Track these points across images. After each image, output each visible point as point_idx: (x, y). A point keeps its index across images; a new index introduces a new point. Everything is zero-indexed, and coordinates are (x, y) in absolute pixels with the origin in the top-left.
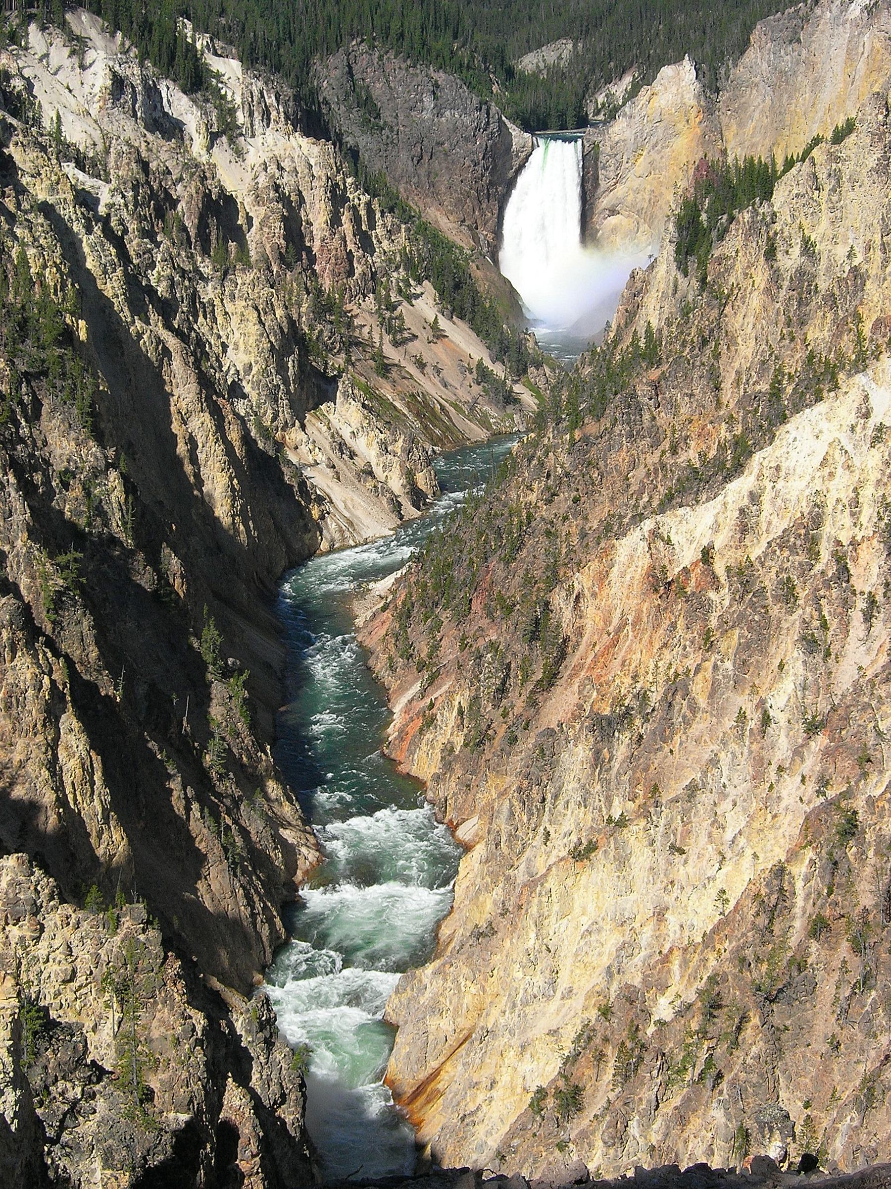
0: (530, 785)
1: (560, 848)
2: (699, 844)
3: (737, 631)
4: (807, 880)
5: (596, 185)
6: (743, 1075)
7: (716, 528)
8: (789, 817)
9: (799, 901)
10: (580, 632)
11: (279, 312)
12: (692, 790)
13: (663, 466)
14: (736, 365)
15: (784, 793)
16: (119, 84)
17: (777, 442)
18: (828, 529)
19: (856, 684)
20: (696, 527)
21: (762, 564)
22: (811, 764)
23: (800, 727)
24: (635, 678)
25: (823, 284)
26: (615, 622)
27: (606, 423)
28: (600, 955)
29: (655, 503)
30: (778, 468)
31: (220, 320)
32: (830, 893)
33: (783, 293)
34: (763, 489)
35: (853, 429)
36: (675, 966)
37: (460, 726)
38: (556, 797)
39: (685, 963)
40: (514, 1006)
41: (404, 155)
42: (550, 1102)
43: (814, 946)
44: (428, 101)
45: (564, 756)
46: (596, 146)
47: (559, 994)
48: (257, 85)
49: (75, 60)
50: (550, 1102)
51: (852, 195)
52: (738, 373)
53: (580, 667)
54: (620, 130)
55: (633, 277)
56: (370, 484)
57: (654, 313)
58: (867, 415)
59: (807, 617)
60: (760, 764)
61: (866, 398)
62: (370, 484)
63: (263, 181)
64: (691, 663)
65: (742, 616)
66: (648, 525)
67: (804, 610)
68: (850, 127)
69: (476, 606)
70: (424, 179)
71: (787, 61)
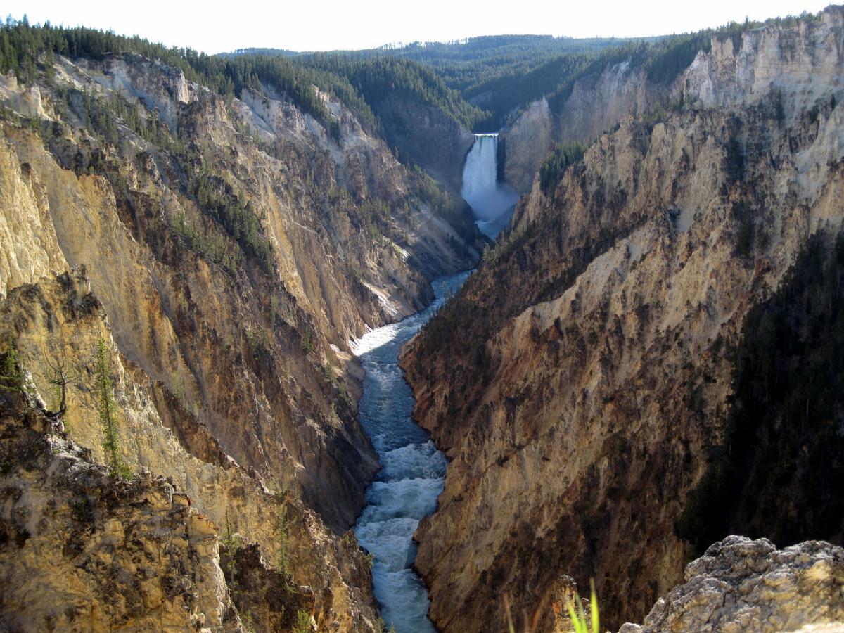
0: (477, 431)
1: (492, 460)
2: (556, 456)
3: (571, 358)
4: (605, 472)
5: (505, 157)
6: (577, 563)
9: (602, 481)
10: (499, 360)
12: (552, 432)
13: (536, 283)
15: (594, 431)
17: (588, 270)
19: (626, 380)
21: (582, 326)
22: (607, 418)
24: (526, 380)
25: (608, 198)
26: (516, 355)
27: (510, 263)
28: (511, 508)
30: (589, 282)
34: (582, 292)
35: (622, 263)
36: (545, 513)
38: (490, 436)
39: (550, 511)
40: (472, 533)
42: (489, 577)
44: (427, 120)
45: (493, 417)
47: (492, 528)
48: (349, 114)
50: (489, 577)
53: (500, 376)
54: (515, 130)
60: (583, 418)
62: (403, 295)
63: (351, 157)
64: (551, 373)
66: (529, 310)
67: (602, 347)
68: (618, 127)
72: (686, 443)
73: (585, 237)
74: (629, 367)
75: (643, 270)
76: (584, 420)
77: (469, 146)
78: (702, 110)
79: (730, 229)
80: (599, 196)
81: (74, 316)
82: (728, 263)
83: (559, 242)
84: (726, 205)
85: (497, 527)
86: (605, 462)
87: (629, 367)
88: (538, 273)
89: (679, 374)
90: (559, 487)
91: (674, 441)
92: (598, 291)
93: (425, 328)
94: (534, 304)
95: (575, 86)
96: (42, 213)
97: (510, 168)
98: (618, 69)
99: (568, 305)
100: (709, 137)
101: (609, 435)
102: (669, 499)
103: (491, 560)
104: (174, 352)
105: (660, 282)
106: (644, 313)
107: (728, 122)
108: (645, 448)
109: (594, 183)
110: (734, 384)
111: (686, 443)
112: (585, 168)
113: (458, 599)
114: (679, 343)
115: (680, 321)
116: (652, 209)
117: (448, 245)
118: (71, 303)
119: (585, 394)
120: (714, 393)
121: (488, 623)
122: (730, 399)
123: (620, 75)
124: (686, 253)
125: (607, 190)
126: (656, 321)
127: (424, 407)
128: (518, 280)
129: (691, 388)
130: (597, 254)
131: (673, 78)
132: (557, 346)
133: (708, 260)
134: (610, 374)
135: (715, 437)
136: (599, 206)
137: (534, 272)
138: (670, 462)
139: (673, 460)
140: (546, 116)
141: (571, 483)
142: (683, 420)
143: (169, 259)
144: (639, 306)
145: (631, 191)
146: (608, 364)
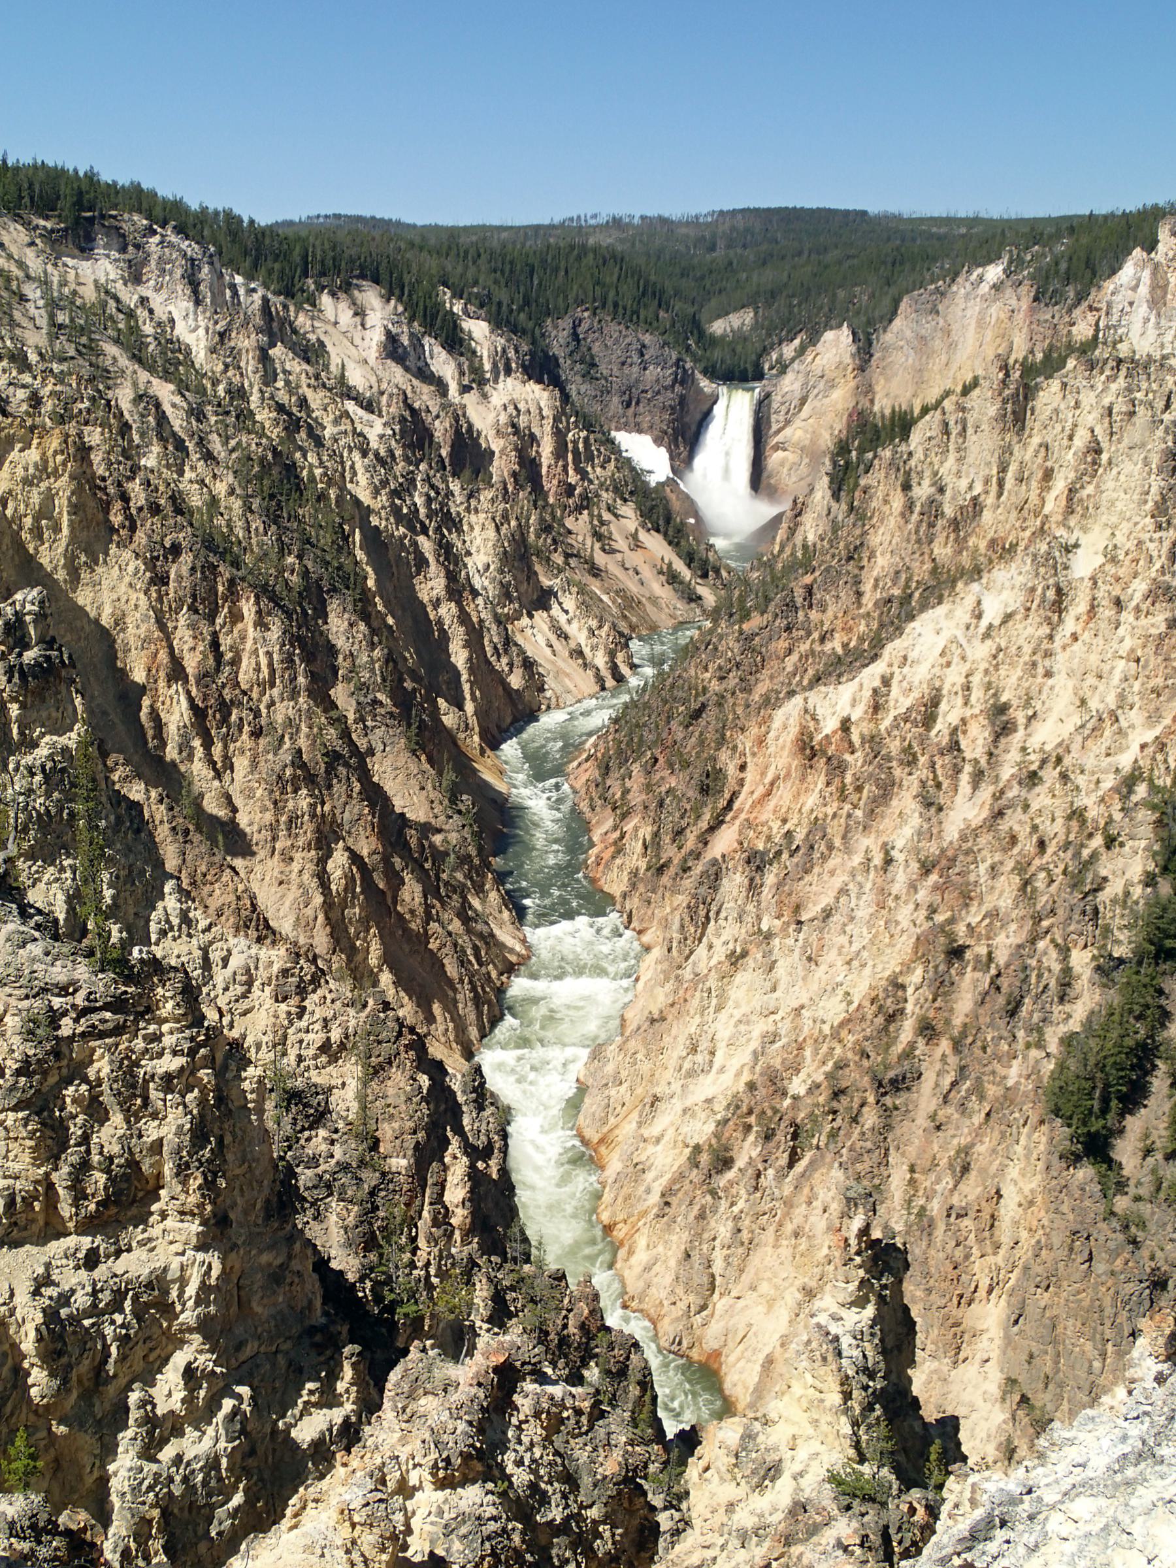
1: (720, 953)
2: (831, 956)
7: (854, 702)
8: (904, 937)
9: (909, 1007)
10: (741, 782)
11: (513, 523)
13: (812, 651)
14: (875, 573)
15: (899, 918)
18: (943, 706)
20: (839, 703)
22: (922, 895)
23: (915, 866)
24: (785, 821)
25: (949, 511)
27: (768, 617)
29: (805, 682)
30: (905, 658)
31: (465, 528)
32: (934, 1000)
33: (915, 517)
34: (892, 674)
35: (968, 628)
36: (808, 1053)
37: (645, 855)
38: (718, 913)
39: (816, 1052)
41: (616, 400)
47: (714, 1069)
50: (704, 1158)
51: (974, 438)
52: (877, 580)
53: (740, 810)
54: (790, 384)
55: (795, 501)
56: (580, 661)
57: (811, 530)
58: (979, 617)
59: (924, 778)
61: (979, 603)
64: (830, 811)
65: (871, 775)
66: (798, 700)
67: (922, 772)
68: (975, 383)
69: (661, 761)
70: (631, 420)
71: (927, 328)
72: (1064, 952)
73: (903, 576)
74: (966, 809)
75: (1003, 645)
77: (705, 408)
78: (1133, 361)
79: (1167, 578)
80: (933, 510)
82: (1161, 637)
83: (858, 582)
84: (1162, 534)
85: (722, 1070)
86: (919, 972)
87: (966, 809)
89: (1059, 826)
90: (833, 1010)
91: (1041, 945)
92: (920, 675)
93: (616, 721)
94: (804, 689)
95: (903, 305)
97: (776, 448)
98: (981, 279)
99: (867, 693)
100: (1141, 410)
101: (927, 925)
102: (1028, 1046)
103: (711, 1127)
105: (1034, 664)
106: (1001, 722)
108: (990, 954)
109: (926, 482)
110: (1155, 854)
112: (910, 454)
114: (1060, 773)
115: (1066, 736)
116: (1028, 533)
117: (663, 578)
119: (886, 849)
120: (1120, 865)
122: (1150, 880)
123: (984, 288)
125: (949, 494)
126: (1021, 733)
127: (607, 855)
128: (782, 645)
129: (1077, 855)
130: (924, 606)
131: (1080, 298)
133: (1121, 631)
134: (934, 820)
135: (1118, 942)
136: (931, 525)
137: (809, 634)
138: (1033, 980)
139: (1040, 976)
140: (848, 360)
141: (855, 1005)
144: (994, 705)
145: (990, 500)
146: (930, 804)
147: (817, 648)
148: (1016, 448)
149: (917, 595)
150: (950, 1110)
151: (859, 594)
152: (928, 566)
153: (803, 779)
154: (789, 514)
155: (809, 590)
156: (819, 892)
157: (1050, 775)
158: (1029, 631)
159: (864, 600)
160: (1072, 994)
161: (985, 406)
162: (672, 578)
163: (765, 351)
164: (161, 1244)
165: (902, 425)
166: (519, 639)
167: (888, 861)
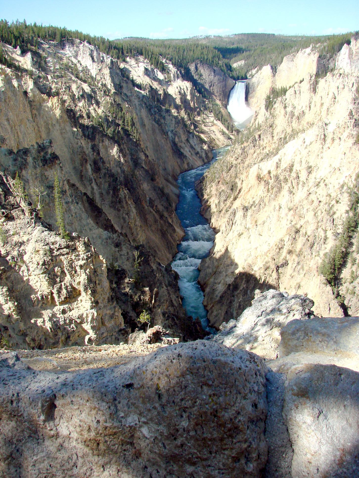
1: (236, 234)
16: (146, 70)
22: (290, 217)
24: (253, 198)
25: (296, 114)
27: (249, 143)
33: (287, 116)
36: (259, 259)
42: (231, 287)
43: (288, 255)
46: (249, 84)
49: (137, 65)
50: (231, 287)
53: (241, 196)
57: (261, 119)
58: (304, 142)
63: (177, 91)
66: (256, 166)
67: (289, 184)
72: (325, 231)
74: (301, 194)
76: (279, 219)
77: (232, 87)
79: (352, 132)
80: (292, 114)
81: (46, 163)
88: (261, 148)
90: (265, 248)
91: (320, 229)
95: (285, 59)
96: (32, 115)
103: (233, 279)
104: (91, 180)
106: (310, 170)
107: (355, 80)
109: (290, 107)
111: (325, 231)
113: (217, 296)
118: (44, 157)
121: (230, 307)
122: (347, 212)
123: (306, 54)
124: (331, 142)
128: (252, 151)
129: (329, 205)
130: (289, 140)
132: (268, 183)
135: (339, 229)
136: (292, 118)
137: (260, 148)
139: (319, 238)
142: (325, 220)
143: (90, 137)
145: (307, 111)
147: (262, 151)
148: (313, 97)
149: (288, 137)
150: (296, 273)
151: (273, 137)
152: (291, 129)
153: (258, 187)
154: (254, 116)
155: (260, 136)
156: (262, 216)
157: (322, 184)
158: (317, 146)
159: (274, 138)
160: (326, 242)
161: (306, 86)
162: (223, 133)
163: (248, 71)
164: (81, 308)
165: (284, 91)
166: (182, 150)
167: (280, 208)
